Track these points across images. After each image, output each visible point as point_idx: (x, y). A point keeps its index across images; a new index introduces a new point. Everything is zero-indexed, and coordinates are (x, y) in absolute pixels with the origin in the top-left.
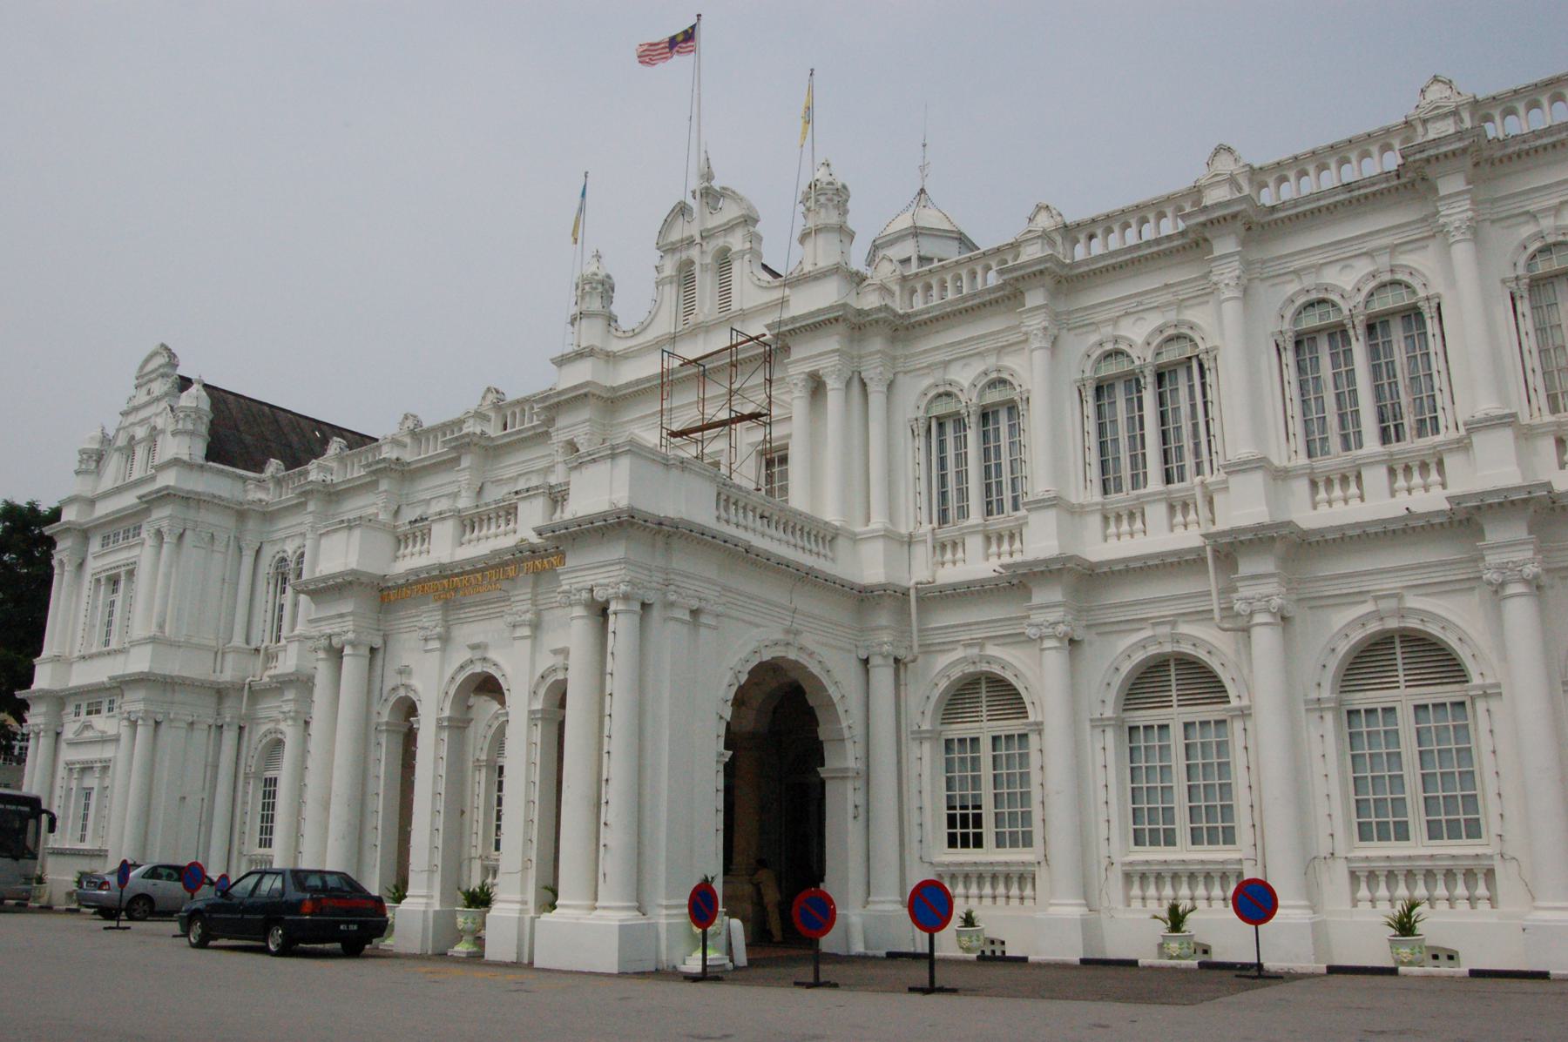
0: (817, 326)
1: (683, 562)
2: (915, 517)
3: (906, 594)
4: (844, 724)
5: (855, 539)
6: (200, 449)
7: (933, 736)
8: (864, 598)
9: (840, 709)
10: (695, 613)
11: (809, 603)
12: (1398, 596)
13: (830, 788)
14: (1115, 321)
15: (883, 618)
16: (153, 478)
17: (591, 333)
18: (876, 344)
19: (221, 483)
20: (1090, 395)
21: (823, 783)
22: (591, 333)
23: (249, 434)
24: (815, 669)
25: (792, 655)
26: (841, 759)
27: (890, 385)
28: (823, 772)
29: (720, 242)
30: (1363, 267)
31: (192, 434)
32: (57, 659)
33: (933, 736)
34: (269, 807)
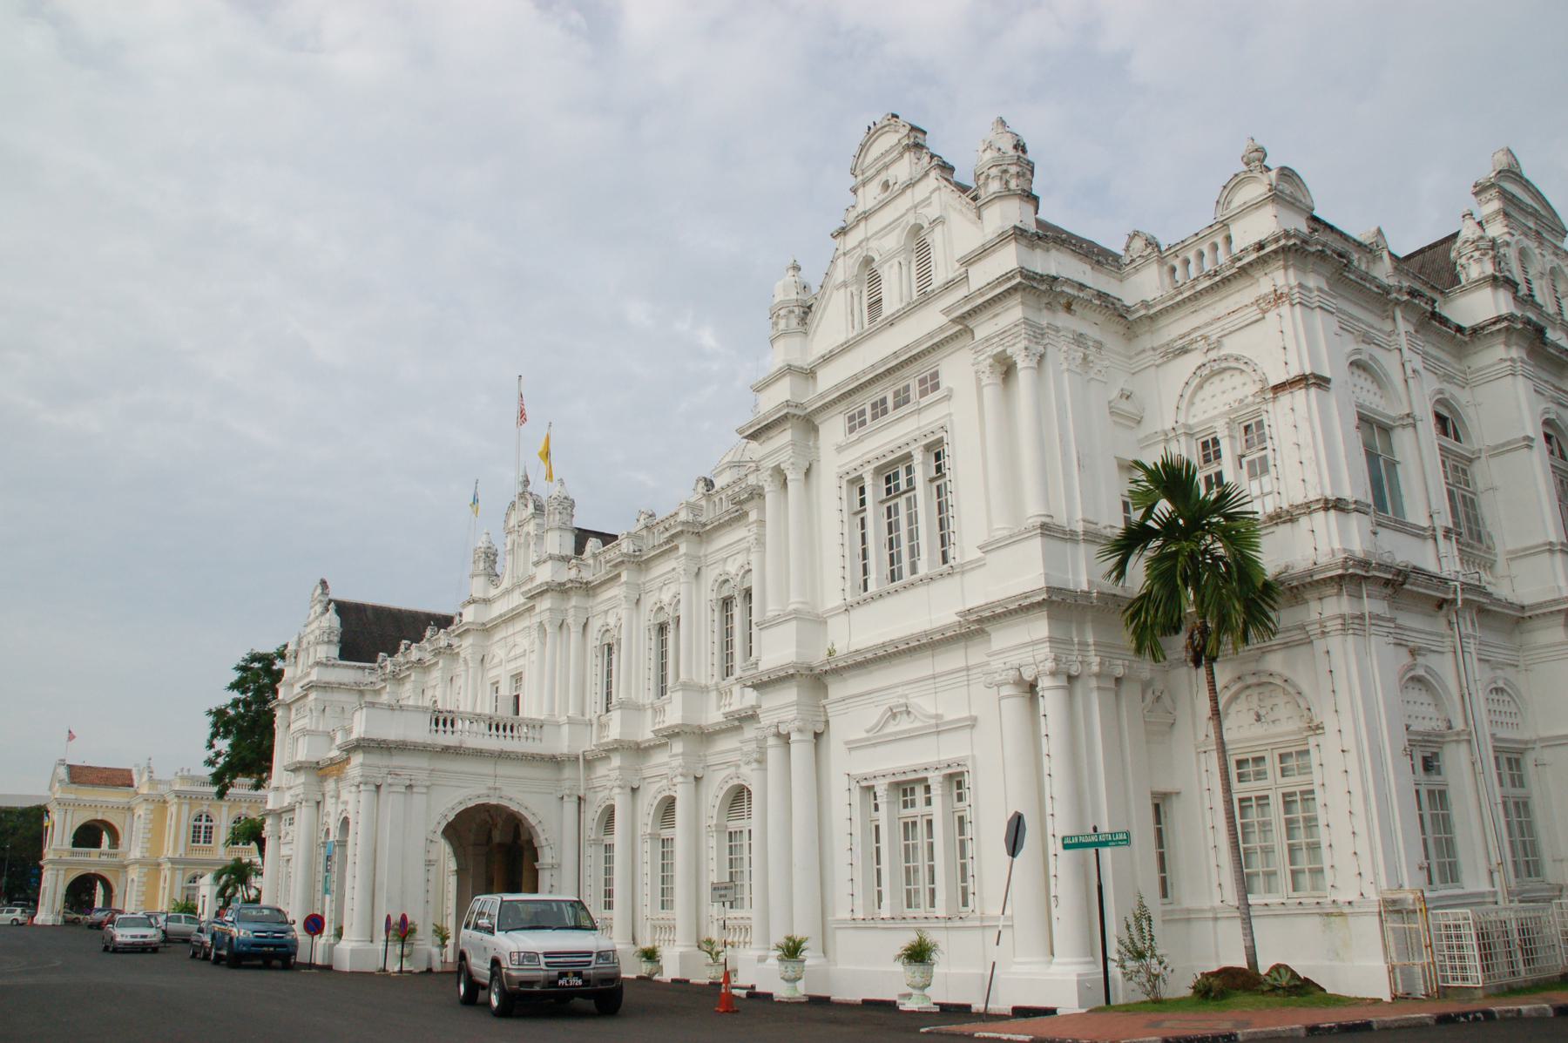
0: (542, 593)
1: (398, 761)
2: (594, 707)
3: (577, 758)
4: (542, 837)
5: (559, 725)
6: (335, 651)
7: (596, 842)
8: (555, 762)
9: (539, 829)
10: (410, 787)
11: (505, 769)
12: (738, 766)
13: (540, 873)
14: (661, 589)
15: (568, 772)
16: (308, 674)
17: (478, 587)
18: (574, 601)
19: (349, 673)
20: (654, 634)
21: (536, 872)
22: (478, 587)
23: (370, 634)
24: (514, 807)
25: (493, 801)
26: (546, 857)
27: (585, 625)
28: (537, 865)
29: (525, 529)
30: (741, 559)
31: (329, 642)
32: (277, 789)
33: (596, 842)
34: (666, 868)
